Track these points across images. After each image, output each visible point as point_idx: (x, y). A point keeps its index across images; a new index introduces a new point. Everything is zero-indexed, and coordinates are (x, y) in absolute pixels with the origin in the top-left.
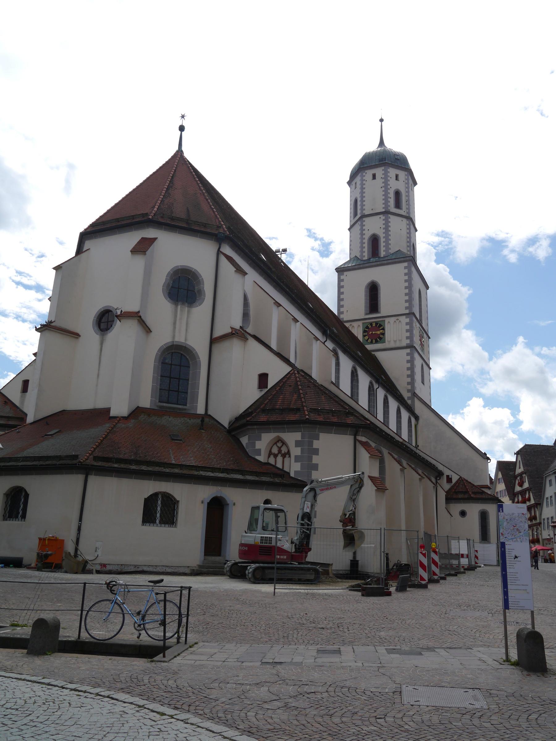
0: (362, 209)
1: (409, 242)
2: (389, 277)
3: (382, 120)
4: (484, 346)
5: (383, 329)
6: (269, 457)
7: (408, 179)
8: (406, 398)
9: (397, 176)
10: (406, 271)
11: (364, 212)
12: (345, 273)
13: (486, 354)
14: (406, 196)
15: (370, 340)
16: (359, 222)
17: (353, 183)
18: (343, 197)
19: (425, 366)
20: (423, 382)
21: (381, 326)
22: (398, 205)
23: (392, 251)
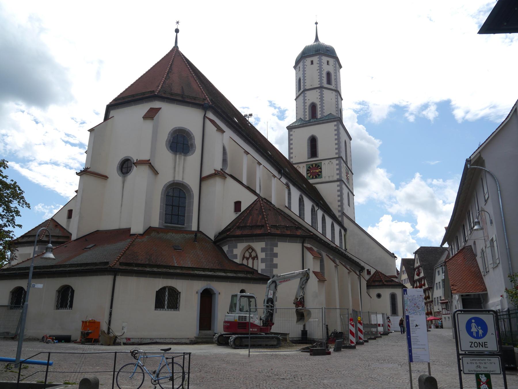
0: (304, 86)
1: (337, 108)
2: (324, 133)
3: (316, 23)
4: (392, 180)
5: (321, 168)
6: (243, 260)
7: (335, 64)
8: (337, 216)
9: (328, 62)
10: (336, 128)
12: (293, 130)
13: (393, 185)
15: (311, 176)
16: (302, 95)
17: (298, 67)
19: (350, 193)
20: (349, 205)
21: (319, 166)
22: (329, 82)
23: (325, 114)
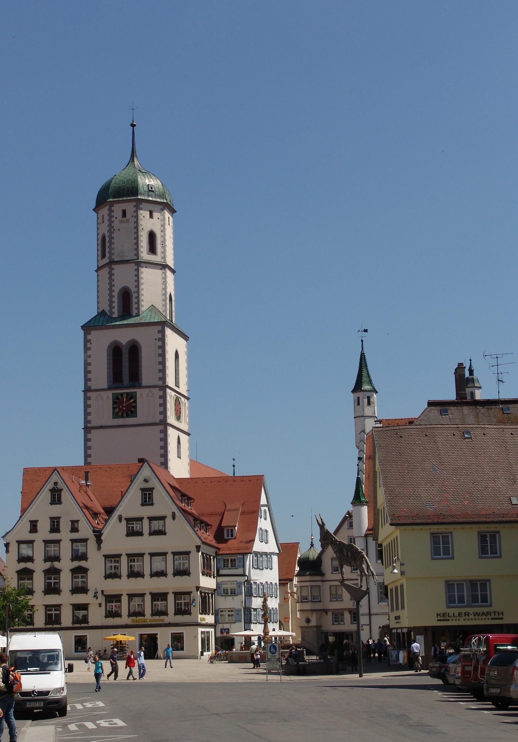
0: (111, 254)
11: (113, 257)
14: (162, 236)
15: (120, 414)
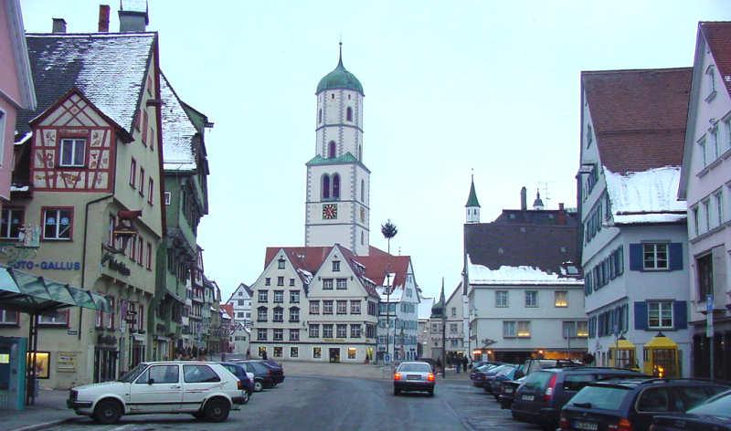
0: (325, 120)
12: (312, 168)
18: (311, 103)
22: (349, 118)
